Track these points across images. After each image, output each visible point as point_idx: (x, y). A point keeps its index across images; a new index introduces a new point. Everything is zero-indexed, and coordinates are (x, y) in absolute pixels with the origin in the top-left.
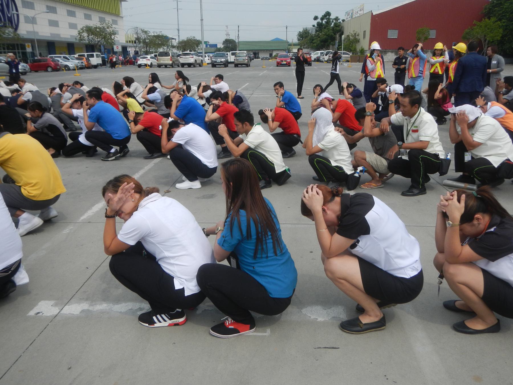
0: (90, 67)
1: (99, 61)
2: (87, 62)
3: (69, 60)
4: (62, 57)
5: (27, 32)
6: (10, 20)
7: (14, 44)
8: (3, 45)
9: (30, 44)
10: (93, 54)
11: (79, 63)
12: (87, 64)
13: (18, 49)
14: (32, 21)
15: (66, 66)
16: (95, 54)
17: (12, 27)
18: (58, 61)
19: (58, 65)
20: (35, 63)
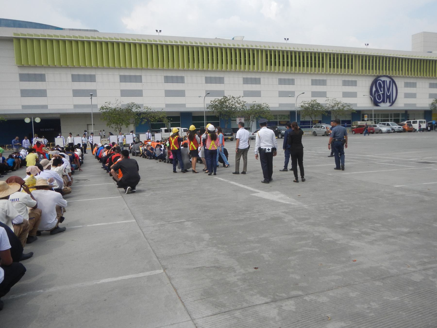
0: (412, 130)
1: (424, 126)
2: (407, 127)
3: (390, 125)
4: (386, 124)
5: (405, 104)
6: (389, 97)
7: (399, 114)
8: (378, 115)
9: (367, 115)
10: (417, 121)
11: (396, 128)
12: (409, 128)
13: (391, 117)
14: (407, 96)
15: (380, 130)
16: (418, 121)
17: (390, 102)
18: (376, 126)
19: (372, 129)
20: (358, 128)
